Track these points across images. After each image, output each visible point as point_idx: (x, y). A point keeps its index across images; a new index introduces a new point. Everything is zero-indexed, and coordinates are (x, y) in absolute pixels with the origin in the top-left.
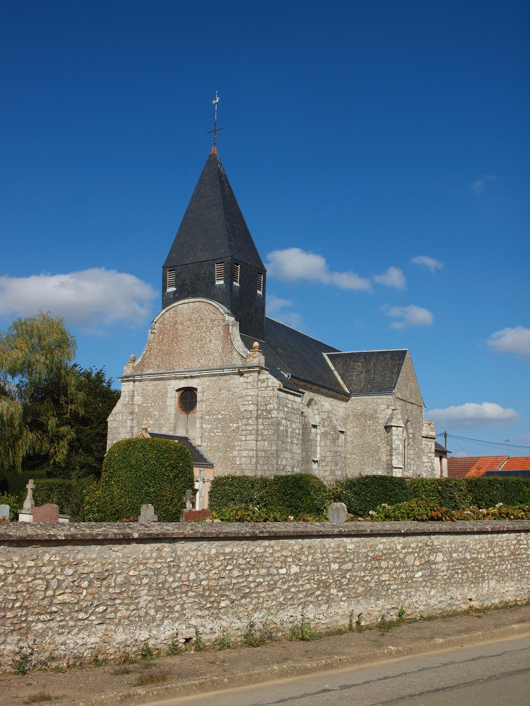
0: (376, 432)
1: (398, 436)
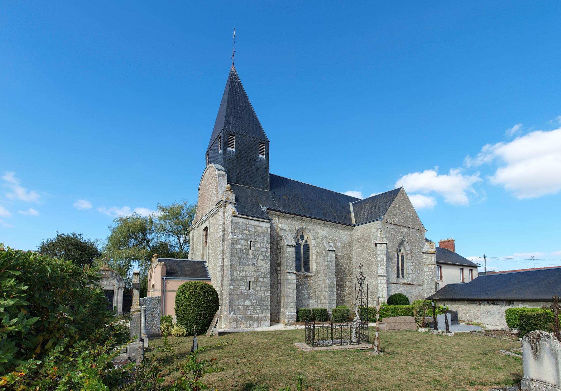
0: (370, 250)
1: (382, 251)
